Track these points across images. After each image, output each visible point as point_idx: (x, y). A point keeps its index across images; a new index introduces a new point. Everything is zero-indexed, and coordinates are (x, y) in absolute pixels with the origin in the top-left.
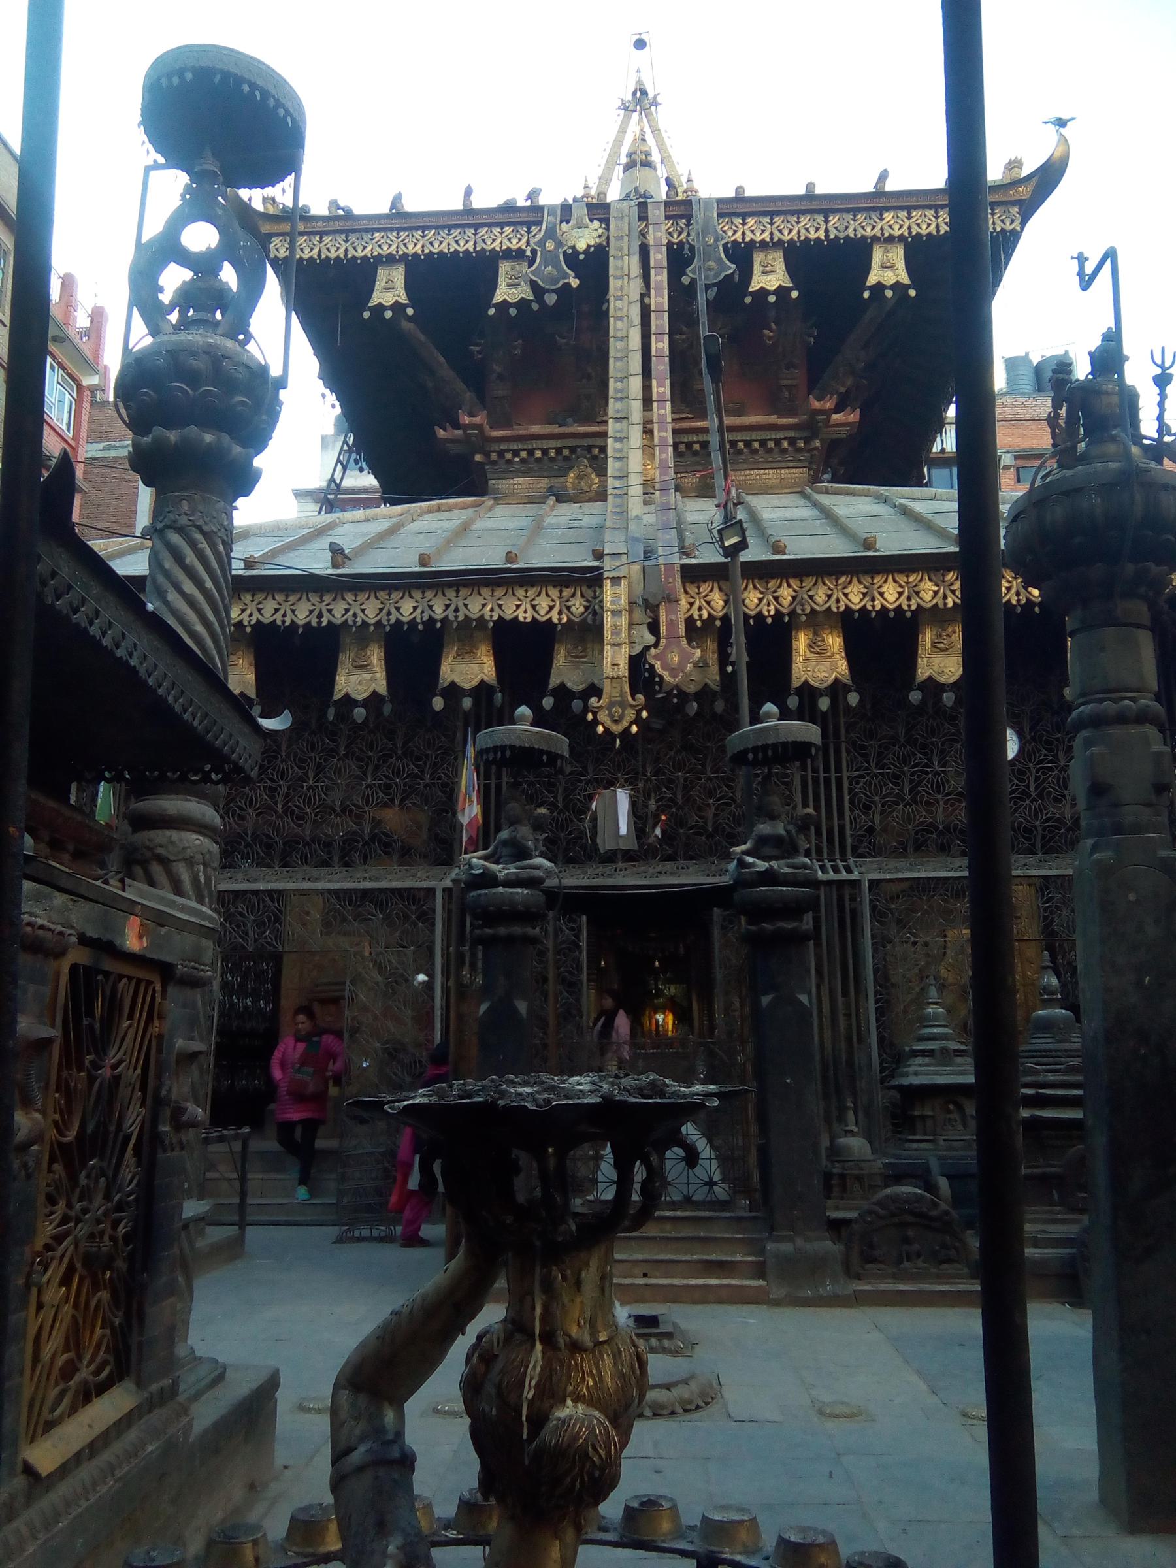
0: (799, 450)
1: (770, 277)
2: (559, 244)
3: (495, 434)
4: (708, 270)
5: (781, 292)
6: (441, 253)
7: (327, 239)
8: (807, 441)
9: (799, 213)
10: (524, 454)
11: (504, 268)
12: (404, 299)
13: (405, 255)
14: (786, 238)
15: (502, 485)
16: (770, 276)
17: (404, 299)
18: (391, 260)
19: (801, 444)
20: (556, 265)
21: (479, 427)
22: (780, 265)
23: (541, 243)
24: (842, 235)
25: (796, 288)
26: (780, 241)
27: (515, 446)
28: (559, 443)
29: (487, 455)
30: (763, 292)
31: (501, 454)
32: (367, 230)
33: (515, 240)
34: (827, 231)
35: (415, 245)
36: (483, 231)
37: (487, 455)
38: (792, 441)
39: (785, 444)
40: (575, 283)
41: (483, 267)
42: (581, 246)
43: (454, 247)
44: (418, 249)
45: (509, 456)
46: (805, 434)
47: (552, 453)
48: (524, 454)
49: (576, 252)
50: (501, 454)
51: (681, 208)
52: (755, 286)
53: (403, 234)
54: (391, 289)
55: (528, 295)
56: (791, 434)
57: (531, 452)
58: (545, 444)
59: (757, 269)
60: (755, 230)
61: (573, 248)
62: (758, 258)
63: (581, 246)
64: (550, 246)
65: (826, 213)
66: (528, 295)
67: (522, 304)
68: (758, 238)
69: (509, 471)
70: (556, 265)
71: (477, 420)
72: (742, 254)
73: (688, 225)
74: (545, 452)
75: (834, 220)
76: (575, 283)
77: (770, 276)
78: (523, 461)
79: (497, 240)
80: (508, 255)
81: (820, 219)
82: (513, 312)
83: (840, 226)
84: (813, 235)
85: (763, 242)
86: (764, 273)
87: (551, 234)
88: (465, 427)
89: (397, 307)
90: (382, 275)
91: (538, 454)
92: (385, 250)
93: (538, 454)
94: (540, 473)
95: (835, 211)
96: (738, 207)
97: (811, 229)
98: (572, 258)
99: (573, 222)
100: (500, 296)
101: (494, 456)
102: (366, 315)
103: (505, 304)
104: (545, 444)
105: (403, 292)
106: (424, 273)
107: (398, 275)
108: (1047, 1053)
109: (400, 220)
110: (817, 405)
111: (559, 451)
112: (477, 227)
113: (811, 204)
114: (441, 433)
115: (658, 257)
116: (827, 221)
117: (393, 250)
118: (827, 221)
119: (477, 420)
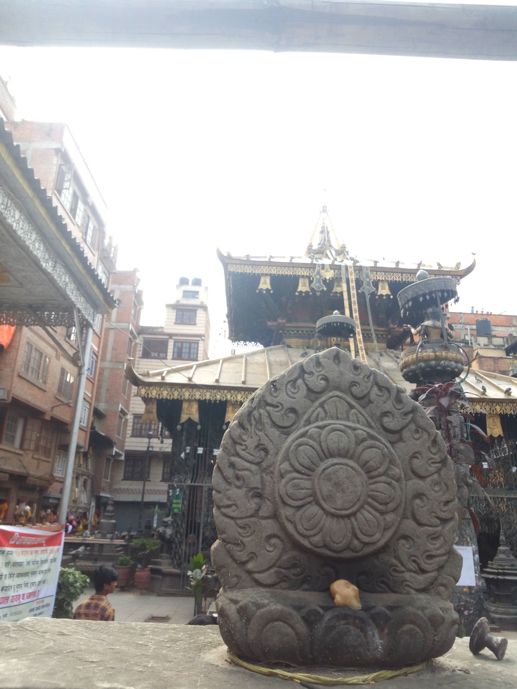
0: (383, 338)
1: (384, 291)
2: (321, 276)
3: (287, 325)
4: (368, 289)
5: (387, 295)
6: (282, 275)
7: (246, 267)
8: (387, 335)
9: (393, 272)
10: (295, 332)
11: (301, 281)
12: (270, 288)
13: (271, 274)
14: (390, 280)
15: (288, 341)
16: (384, 291)
17: (270, 288)
18: (266, 275)
19: (384, 336)
20: (320, 283)
21: (283, 324)
22: (387, 287)
23: (315, 276)
24: (407, 280)
25: (392, 295)
26: (388, 281)
27: (293, 329)
28: (307, 329)
29: (284, 331)
30: (382, 295)
31: (288, 331)
32: (259, 265)
33: (306, 273)
34: (402, 279)
35: (274, 271)
36: (295, 269)
37: (284, 331)
38: (382, 335)
39: (379, 336)
40: (325, 289)
41: (295, 280)
42: (328, 278)
43: (286, 273)
44: (275, 273)
45: (290, 332)
46: (386, 333)
47: (305, 332)
48: (295, 332)
49: (326, 279)
50: (288, 331)
51: (359, 269)
52: (379, 293)
53: (270, 267)
54: (265, 284)
55: (309, 290)
56: (382, 333)
57: (298, 331)
58: (303, 329)
59: (380, 288)
60: (380, 277)
61: (325, 278)
62: (380, 285)
63: (328, 278)
64: (318, 277)
65: (402, 273)
66: (309, 290)
67: (307, 292)
68: (381, 279)
69: (290, 337)
70: (320, 283)
71: (284, 321)
72: (376, 284)
73: (359, 273)
74: (302, 331)
75: (404, 275)
76: (325, 289)
77: (384, 291)
78: (295, 334)
79: (300, 272)
80: (303, 276)
81: (400, 274)
82: (303, 294)
83: (405, 278)
84: (398, 280)
85: (382, 280)
86: (382, 289)
87: (318, 273)
88: (279, 323)
89: (267, 290)
90: (263, 279)
91: (300, 332)
92: (265, 272)
93: (300, 332)
94: (300, 337)
95: (405, 273)
96: (375, 269)
97: (397, 278)
98: (325, 281)
99: (325, 270)
100: (300, 289)
101: (286, 332)
102: (257, 291)
103: (301, 292)
104: (303, 329)
105: (269, 285)
106: (275, 280)
107: (268, 280)
108: (504, 560)
109: (270, 264)
110: (392, 326)
111: (307, 331)
112: (293, 267)
113: (396, 270)
114: (270, 323)
115: (353, 284)
116: (402, 275)
117: (267, 272)
118: (402, 275)
119: (284, 321)
